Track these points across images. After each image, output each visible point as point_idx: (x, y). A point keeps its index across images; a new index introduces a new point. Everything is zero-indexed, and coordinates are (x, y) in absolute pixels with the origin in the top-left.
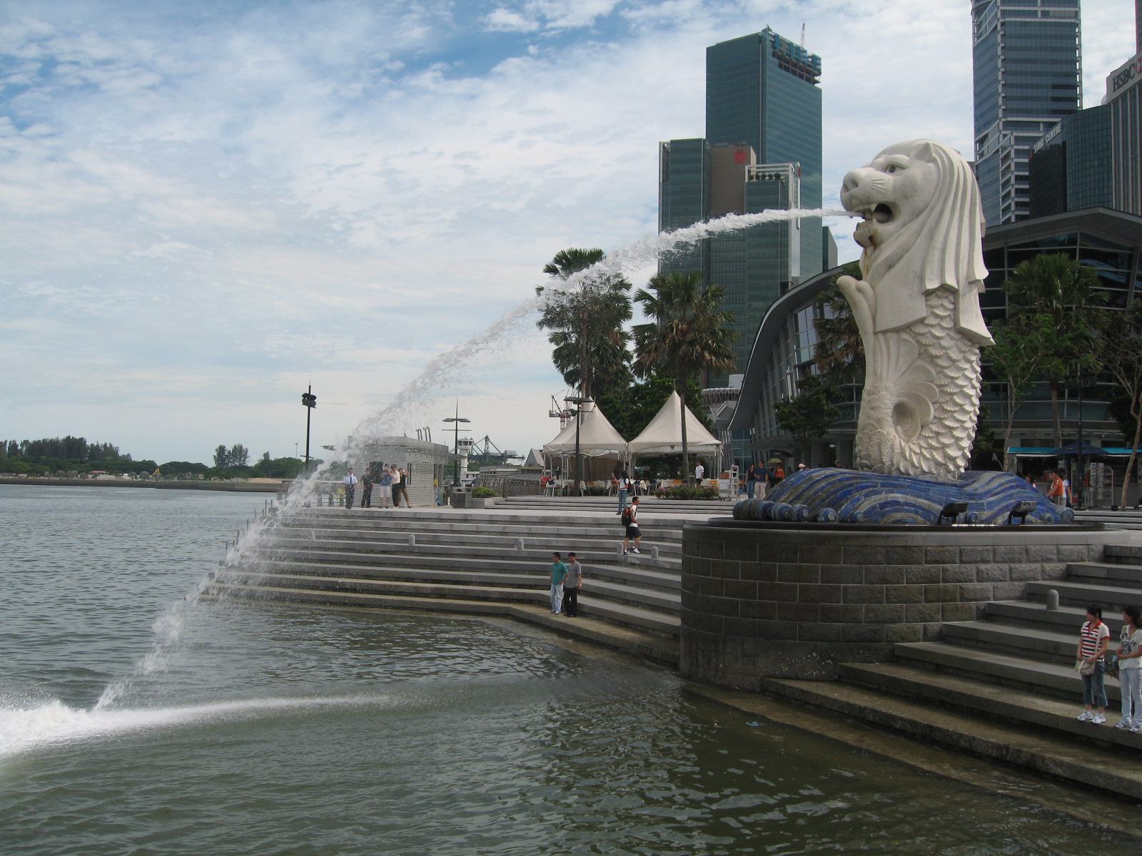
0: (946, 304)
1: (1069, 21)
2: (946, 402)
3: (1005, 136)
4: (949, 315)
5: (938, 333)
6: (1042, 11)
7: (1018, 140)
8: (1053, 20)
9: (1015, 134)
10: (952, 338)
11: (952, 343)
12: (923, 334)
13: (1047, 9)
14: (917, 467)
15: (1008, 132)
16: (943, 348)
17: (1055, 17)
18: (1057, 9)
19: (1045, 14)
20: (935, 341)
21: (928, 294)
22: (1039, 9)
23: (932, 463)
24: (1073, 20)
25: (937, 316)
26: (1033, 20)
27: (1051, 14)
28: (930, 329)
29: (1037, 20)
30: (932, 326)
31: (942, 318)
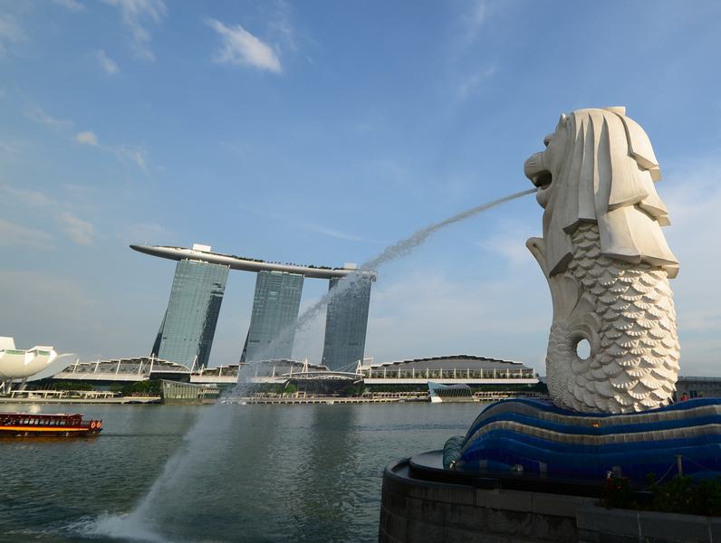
0: (590, 235)
2: (608, 329)
4: (595, 245)
5: (585, 263)
10: (602, 266)
11: (602, 270)
12: (575, 269)
14: (581, 402)
16: (593, 277)
20: (584, 272)
21: (571, 231)
23: (595, 396)
25: (583, 249)
28: (580, 263)
30: (580, 259)
31: (588, 249)
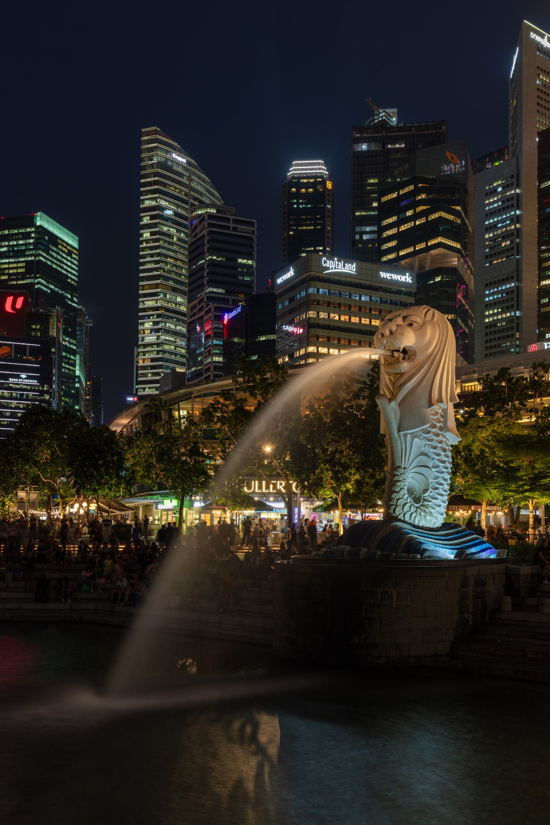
1: (249, 235)
3: (208, 305)
6: (233, 227)
7: (215, 307)
8: (239, 234)
9: (215, 305)
13: (236, 226)
15: (210, 303)
17: (240, 232)
18: (242, 227)
19: (235, 229)
22: (232, 225)
24: (252, 236)
26: (227, 232)
27: (239, 230)
29: (230, 232)
